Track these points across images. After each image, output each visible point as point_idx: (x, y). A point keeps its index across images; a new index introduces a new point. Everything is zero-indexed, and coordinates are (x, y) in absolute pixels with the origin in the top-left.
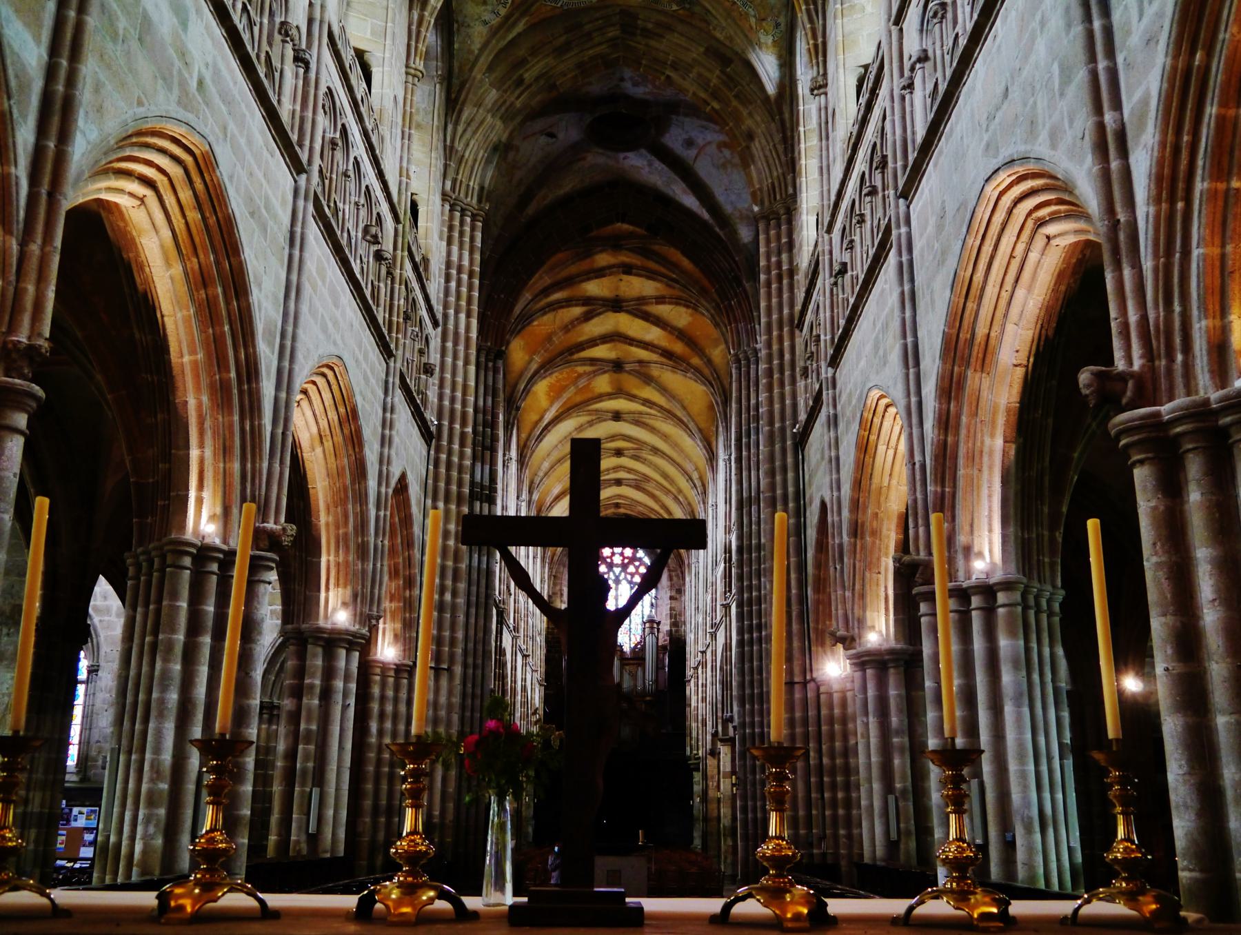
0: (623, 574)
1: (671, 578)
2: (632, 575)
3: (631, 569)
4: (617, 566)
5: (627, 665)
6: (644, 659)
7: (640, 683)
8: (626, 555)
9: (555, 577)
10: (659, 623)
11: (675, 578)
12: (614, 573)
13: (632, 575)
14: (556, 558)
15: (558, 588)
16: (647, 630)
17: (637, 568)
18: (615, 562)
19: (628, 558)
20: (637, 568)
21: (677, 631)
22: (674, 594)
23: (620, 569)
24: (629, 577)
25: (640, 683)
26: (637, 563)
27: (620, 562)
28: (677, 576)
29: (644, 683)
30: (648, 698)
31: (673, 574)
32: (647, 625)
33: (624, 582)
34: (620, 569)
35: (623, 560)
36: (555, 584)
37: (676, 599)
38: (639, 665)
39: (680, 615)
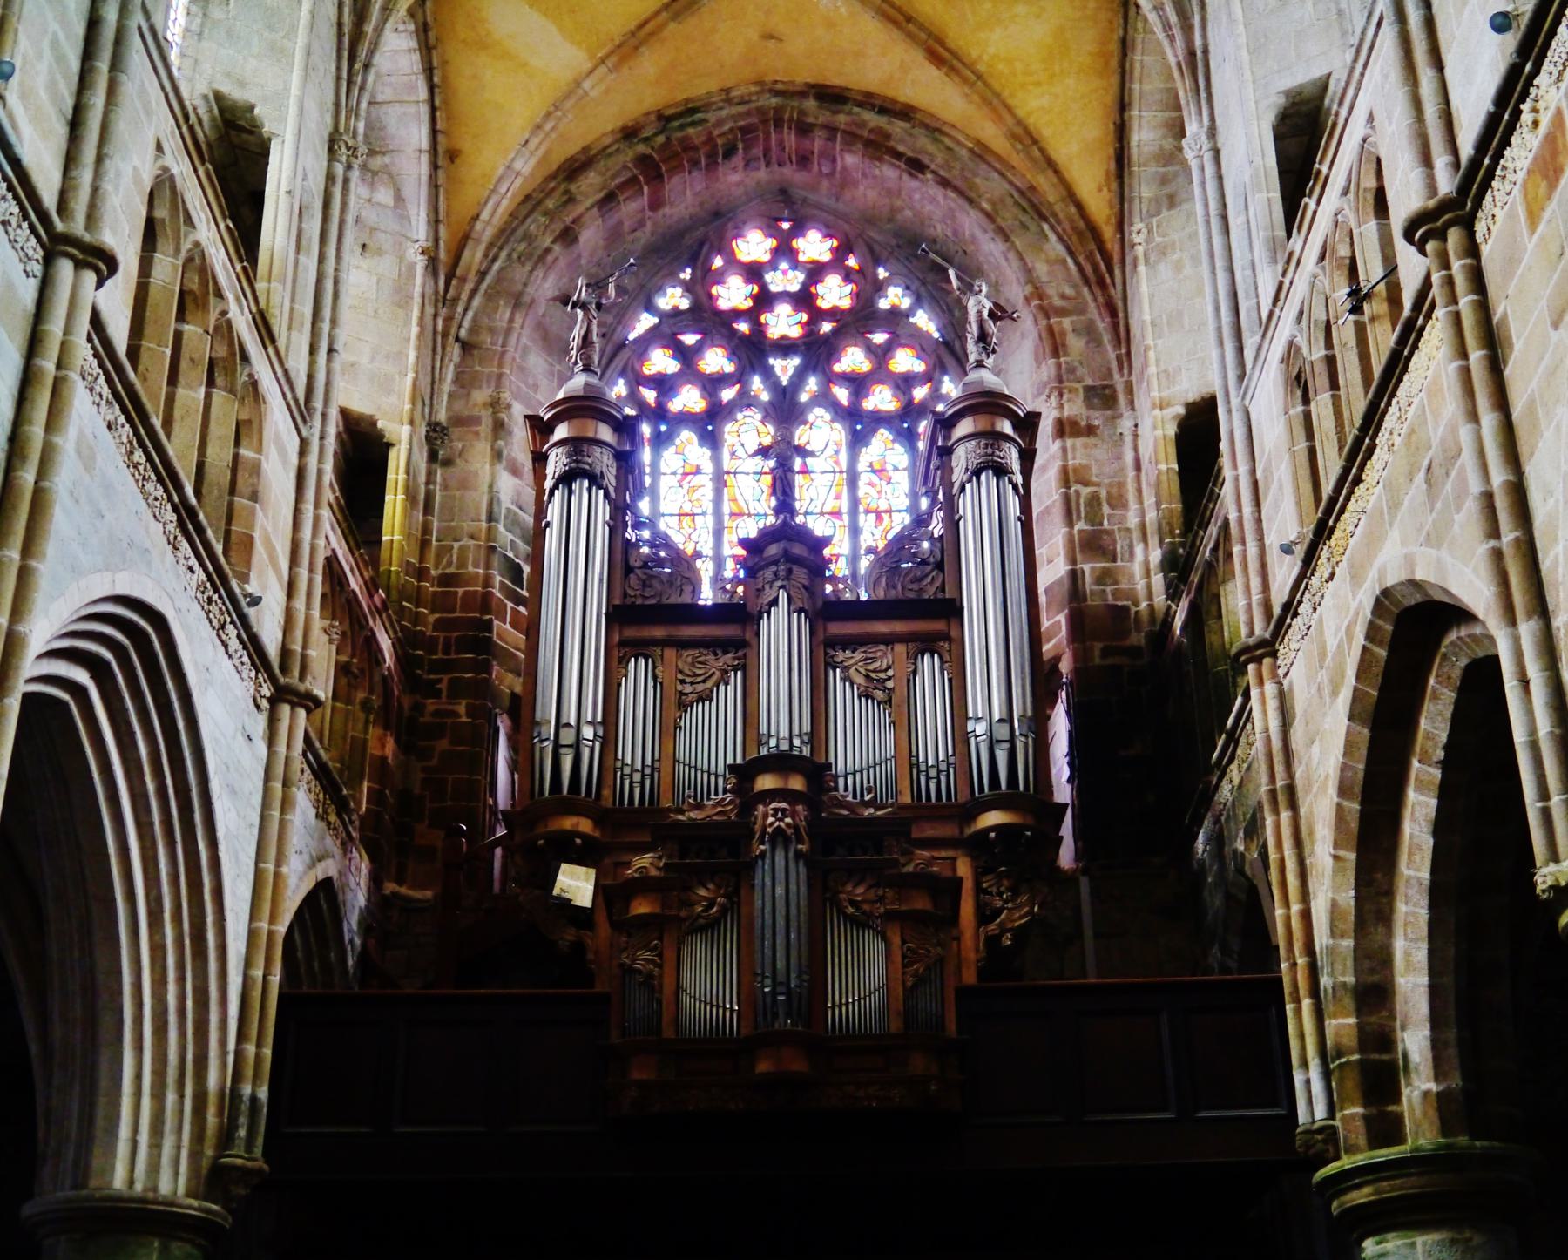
0: (812, 384)
1: (1055, 344)
2: (859, 384)
3: (853, 359)
4: (785, 347)
5: (852, 643)
6: (952, 610)
7: (933, 743)
8: (824, 304)
9: (467, 347)
10: (1028, 424)
11: (1076, 344)
12: (768, 374)
13: (859, 384)
14: (473, 256)
15: (481, 396)
16: (963, 458)
17: (881, 356)
18: (774, 333)
19: (833, 313)
20: (881, 356)
21: (1104, 577)
22: (1075, 408)
23: (795, 361)
24: (842, 394)
25: (933, 743)
26: (879, 338)
27: (795, 332)
28: (1089, 332)
29: (961, 737)
30: (992, 818)
31: (1067, 323)
32: (965, 427)
33: (819, 414)
34: (795, 361)
35: (810, 326)
36: (465, 381)
37: (1090, 431)
38: (926, 644)
39: (1118, 501)
